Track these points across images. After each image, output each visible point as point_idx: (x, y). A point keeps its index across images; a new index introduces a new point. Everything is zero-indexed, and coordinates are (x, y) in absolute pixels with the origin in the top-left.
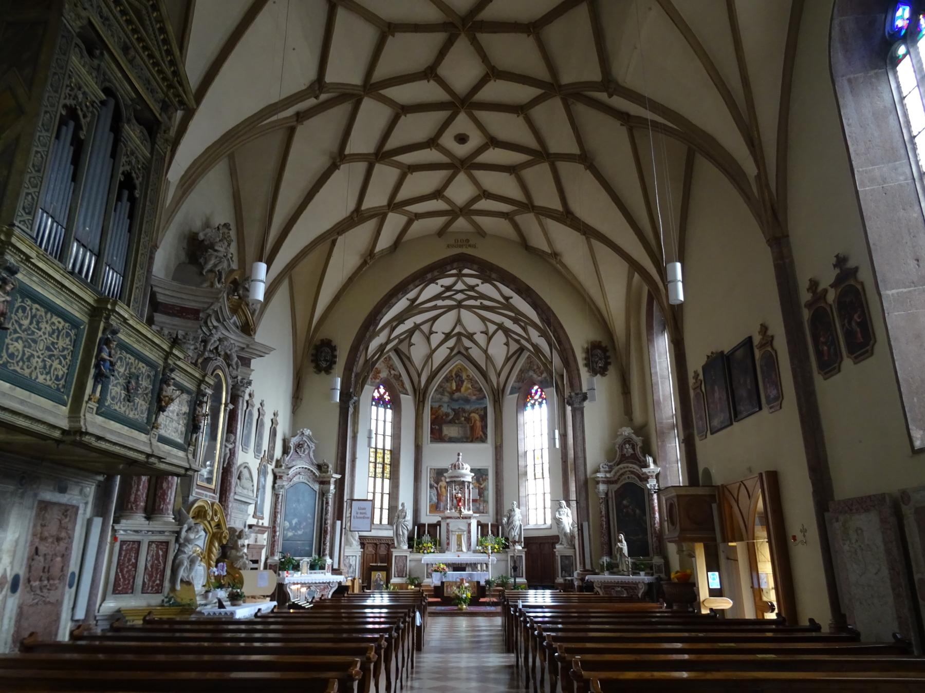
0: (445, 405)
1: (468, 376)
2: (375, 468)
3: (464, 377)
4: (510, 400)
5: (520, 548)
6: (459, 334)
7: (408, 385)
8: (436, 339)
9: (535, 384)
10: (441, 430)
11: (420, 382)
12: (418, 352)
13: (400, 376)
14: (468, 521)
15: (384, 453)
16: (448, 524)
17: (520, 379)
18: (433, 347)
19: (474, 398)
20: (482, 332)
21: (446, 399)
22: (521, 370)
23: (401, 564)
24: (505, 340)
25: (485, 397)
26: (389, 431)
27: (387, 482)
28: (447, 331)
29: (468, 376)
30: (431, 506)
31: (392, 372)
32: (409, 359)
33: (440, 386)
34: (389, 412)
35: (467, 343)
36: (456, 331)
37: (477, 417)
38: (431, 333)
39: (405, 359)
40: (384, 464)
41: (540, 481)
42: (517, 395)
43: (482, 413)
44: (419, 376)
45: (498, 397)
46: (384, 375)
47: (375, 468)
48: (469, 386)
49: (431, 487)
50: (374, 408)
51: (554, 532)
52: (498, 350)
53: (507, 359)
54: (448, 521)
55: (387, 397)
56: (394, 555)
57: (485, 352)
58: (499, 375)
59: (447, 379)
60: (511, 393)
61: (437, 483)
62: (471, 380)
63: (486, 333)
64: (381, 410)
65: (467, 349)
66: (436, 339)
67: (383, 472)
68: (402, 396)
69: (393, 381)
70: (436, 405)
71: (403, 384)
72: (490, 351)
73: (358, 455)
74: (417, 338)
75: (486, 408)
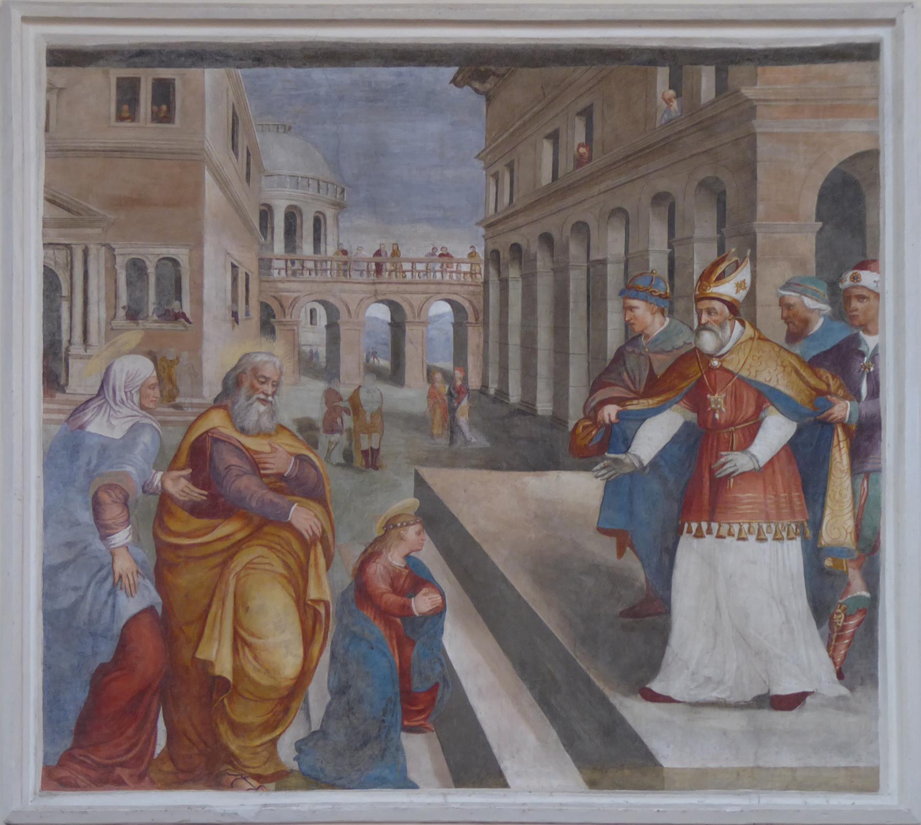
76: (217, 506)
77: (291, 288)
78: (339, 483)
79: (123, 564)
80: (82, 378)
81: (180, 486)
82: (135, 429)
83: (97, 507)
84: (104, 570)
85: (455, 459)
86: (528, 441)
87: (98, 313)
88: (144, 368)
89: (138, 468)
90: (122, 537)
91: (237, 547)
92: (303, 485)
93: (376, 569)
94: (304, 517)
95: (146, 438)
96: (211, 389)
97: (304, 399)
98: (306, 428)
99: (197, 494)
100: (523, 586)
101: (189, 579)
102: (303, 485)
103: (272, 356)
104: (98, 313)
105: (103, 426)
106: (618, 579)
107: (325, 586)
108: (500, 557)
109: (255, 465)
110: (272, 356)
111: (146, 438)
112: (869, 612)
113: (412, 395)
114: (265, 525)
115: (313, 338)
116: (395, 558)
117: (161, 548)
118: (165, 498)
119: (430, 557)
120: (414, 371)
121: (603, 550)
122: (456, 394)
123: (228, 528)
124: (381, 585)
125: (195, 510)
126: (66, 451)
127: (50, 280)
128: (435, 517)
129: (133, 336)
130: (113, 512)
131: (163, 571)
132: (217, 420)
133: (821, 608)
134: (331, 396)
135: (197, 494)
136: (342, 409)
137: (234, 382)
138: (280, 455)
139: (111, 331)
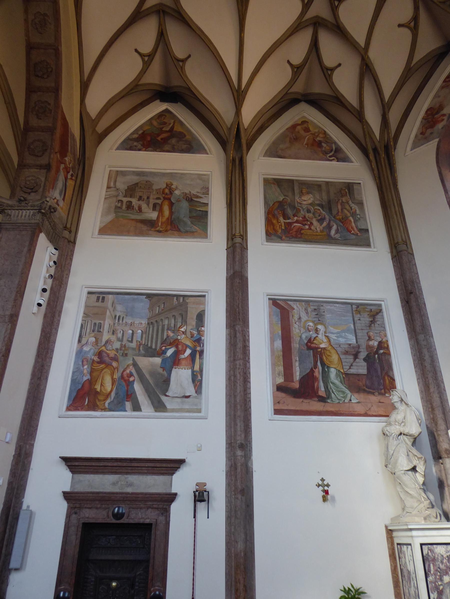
76: (101, 362)
77: (117, 327)
78: (121, 358)
79: (85, 371)
80: (84, 341)
81: (96, 359)
82: (91, 349)
83: (83, 361)
84: (82, 372)
85: (139, 355)
86: (151, 352)
87: (88, 330)
88: (94, 339)
89: (90, 356)
90: (86, 367)
91: (104, 368)
92: (115, 359)
93: (125, 373)
94: (114, 364)
95: (92, 351)
96: (103, 343)
97: (117, 345)
98: (117, 349)
99: (99, 360)
100: (147, 376)
101: (95, 374)
102: (115, 359)
103: (113, 338)
104: (88, 330)
105: (86, 349)
106: (162, 375)
107: (116, 376)
108: (144, 371)
109: (108, 355)
110: (113, 338)
111: (92, 351)
112: (201, 381)
113: (134, 345)
114: (108, 365)
115: (120, 335)
116: (128, 371)
117: (92, 369)
118: (93, 360)
119: (134, 371)
120: (134, 341)
121: (161, 370)
122: (140, 344)
123: (103, 366)
124: (125, 376)
125: (98, 363)
126: (79, 352)
127: (82, 325)
128: (135, 365)
129: (93, 334)
130: (85, 363)
131: (91, 373)
132: (103, 348)
133: (194, 381)
134: (121, 345)
135: (99, 360)
136: (123, 347)
137: (107, 342)
138: (112, 354)
139: (90, 334)
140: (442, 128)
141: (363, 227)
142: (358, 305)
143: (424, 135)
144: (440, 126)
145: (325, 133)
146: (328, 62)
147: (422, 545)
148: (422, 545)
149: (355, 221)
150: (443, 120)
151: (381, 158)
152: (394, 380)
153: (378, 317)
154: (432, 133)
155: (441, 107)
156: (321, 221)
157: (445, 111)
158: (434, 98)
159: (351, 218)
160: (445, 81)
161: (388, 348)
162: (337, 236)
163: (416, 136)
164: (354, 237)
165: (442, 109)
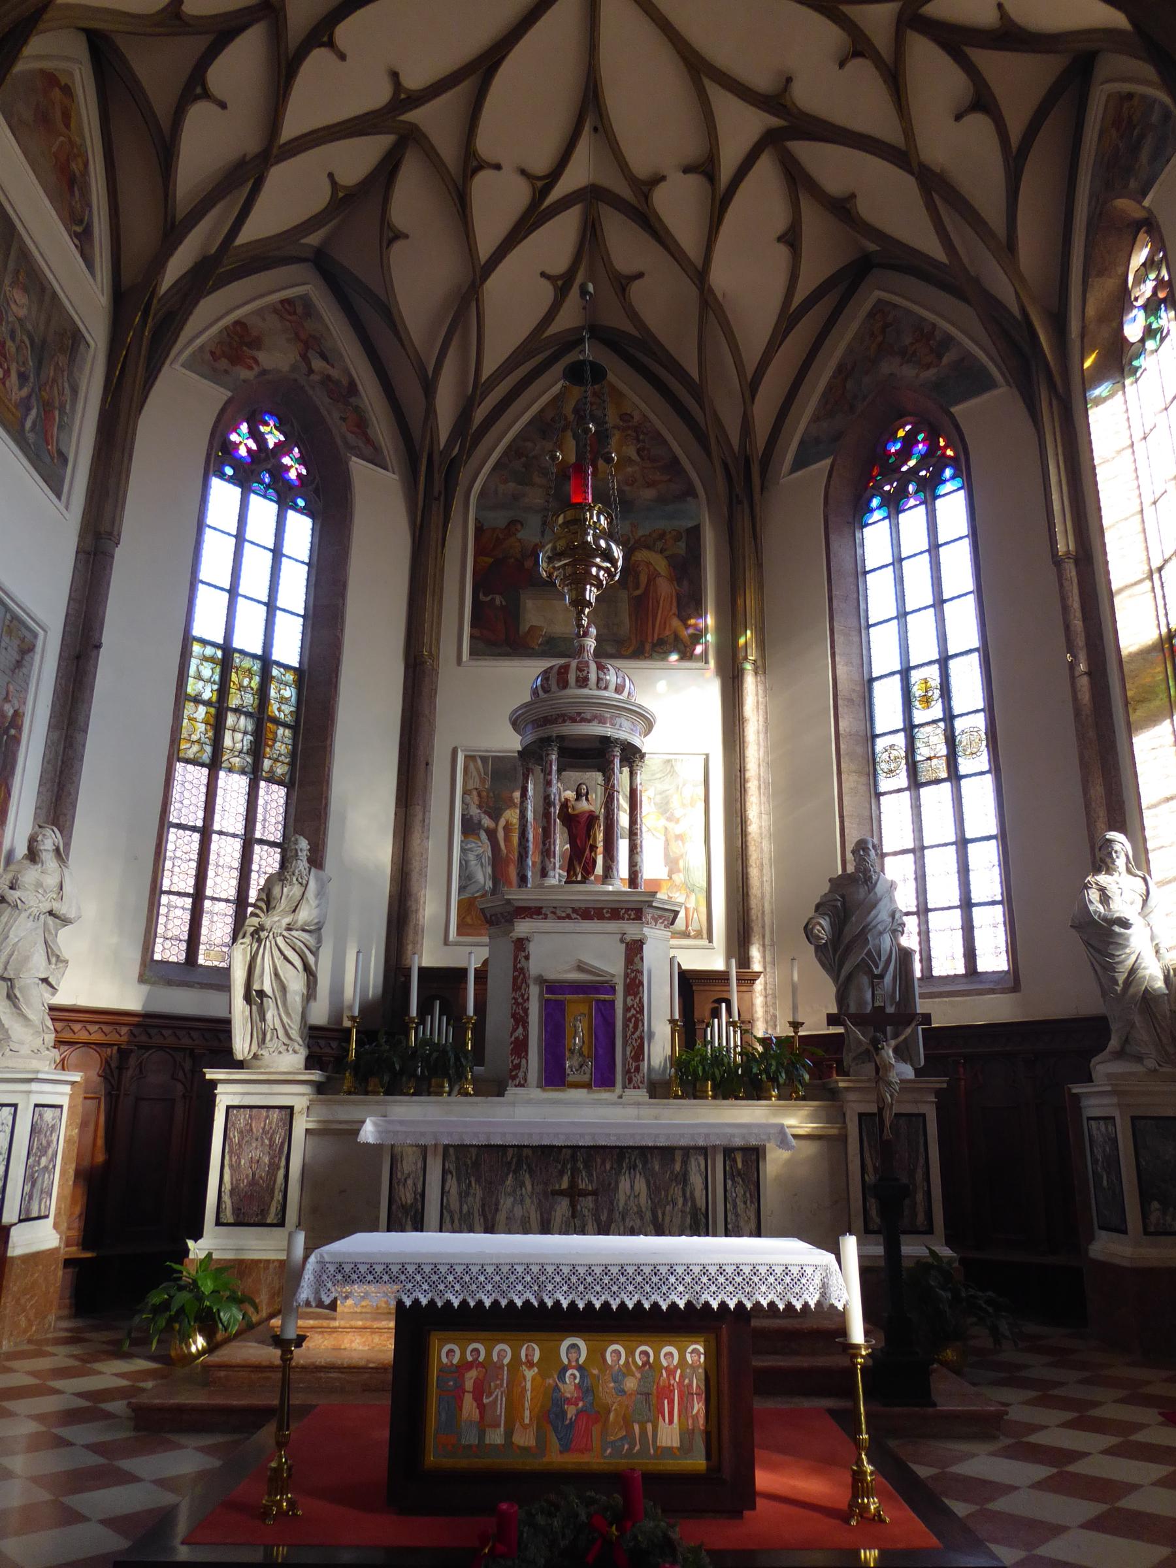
0: (534, 521)
1: (625, 417)
2: (217, 725)
3: (612, 418)
4: (800, 490)
5: (908, 1071)
6: (592, 195)
7: (382, 429)
8: (497, 201)
9: (899, 417)
10: (513, 613)
11: (430, 411)
12: (418, 280)
13: (352, 389)
14: (632, 930)
15: (266, 678)
16: (521, 945)
17: (837, 400)
18: (485, 248)
19: (649, 494)
20: (687, 170)
21: (535, 497)
22: (840, 369)
23: (256, 1152)
24: (779, 220)
25: (696, 496)
26: (294, 589)
27: (273, 798)
28: (541, 165)
29: (625, 417)
30: (466, 907)
31: (317, 364)
32: (388, 313)
33: (514, 451)
34: (300, 530)
35: (625, 246)
36: (574, 179)
37: (661, 564)
38: (473, 164)
39: (368, 308)
40: (261, 716)
41: (937, 798)
42: (828, 461)
43: (681, 548)
44: (429, 388)
45: (744, 486)
46: (278, 357)
47: (217, 725)
48: (631, 451)
49: (470, 827)
50: (223, 497)
51: (1063, 997)
52: (752, 273)
53: (787, 321)
54: (523, 928)
55: (293, 467)
56: (225, 1097)
57: (700, 275)
58: (752, 387)
59: (544, 427)
60: (800, 463)
61: (495, 815)
62: (637, 431)
63: (706, 167)
64: (263, 510)
65: (622, 283)
66: (497, 201)
67: (257, 751)
68: (359, 468)
69: (321, 399)
70: (498, 519)
71: (361, 425)
72: (721, 277)
73: (111, 635)
74: (412, 200)
75: (694, 534)
140: (244, 381)
141: (64, 450)
142: (15, 618)
143: (215, 361)
144: (245, 374)
145: (86, 165)
146: (218, 76)
147: (15, 1106)
148: (15, 1106)
149: (60, 427)
150: (250, 368)
151: (144, 329)
152: (10, 796)
153: (27, 657)
154: (226, 372)
155: (256, 343)
156: (23, 377)
157: (261, 356)
158: (253, 313)
159: (57, 413)
160: (282, 302)
161: (19, 729)
162: (31, 437)
163: (201, 348)
164: (48, 460)
165: (259, 349)
